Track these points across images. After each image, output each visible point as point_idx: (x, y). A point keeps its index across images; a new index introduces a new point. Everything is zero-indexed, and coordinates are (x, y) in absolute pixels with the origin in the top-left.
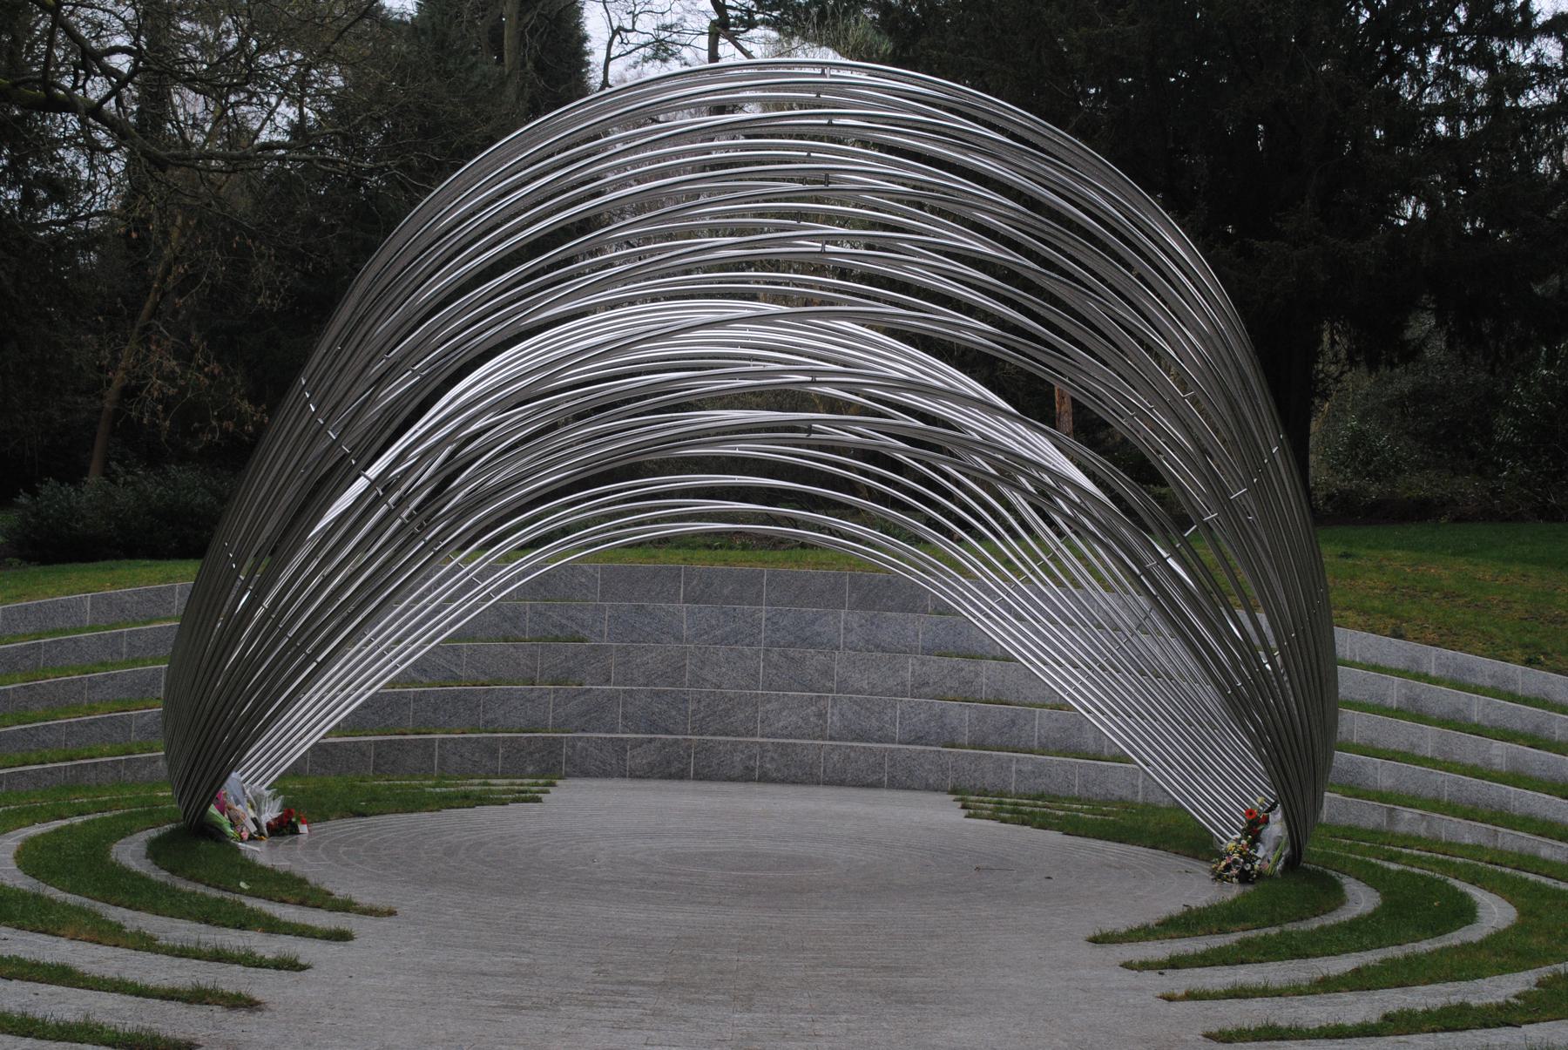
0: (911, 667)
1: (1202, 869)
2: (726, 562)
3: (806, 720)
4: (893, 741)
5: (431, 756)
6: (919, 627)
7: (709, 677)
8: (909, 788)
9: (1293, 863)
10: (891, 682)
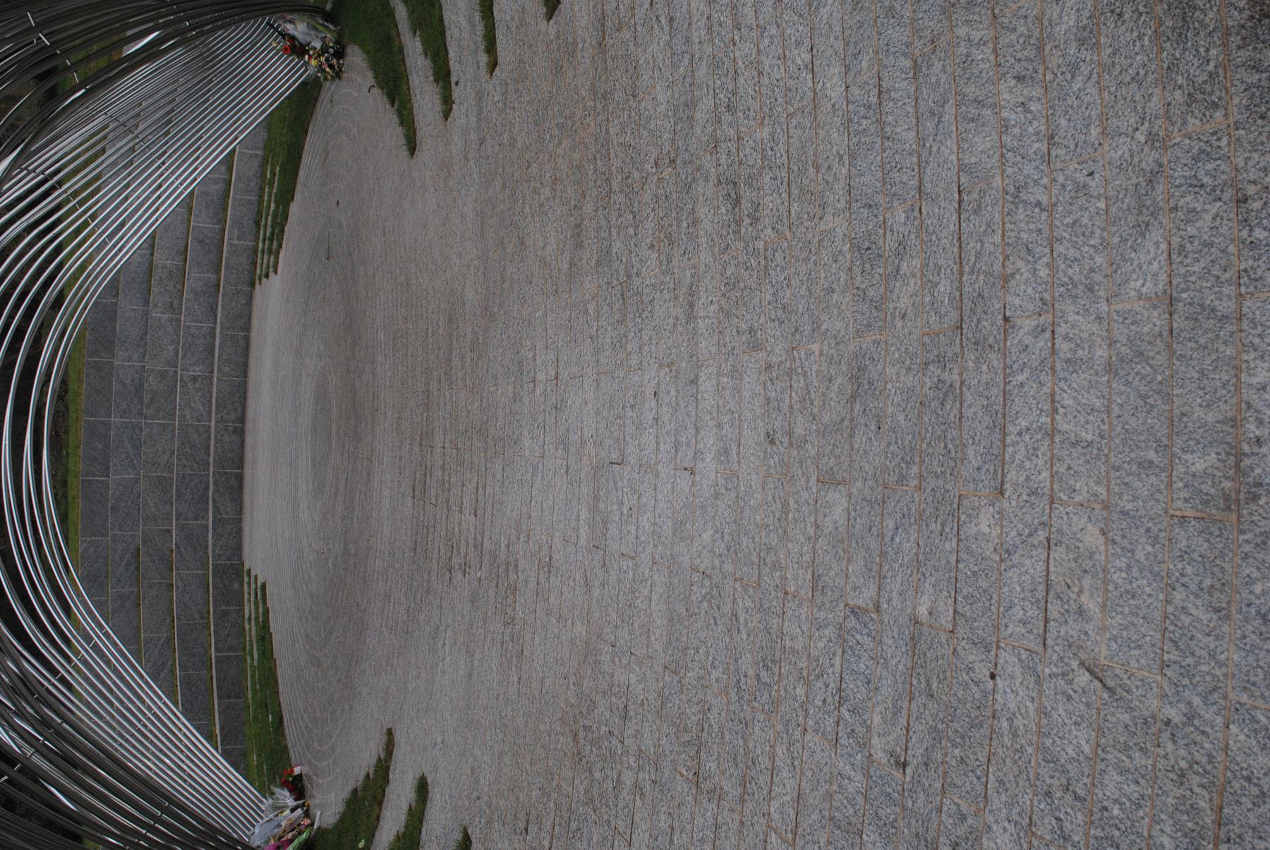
0: (158, 314)
1: (330, 90)
2: (77, 447)
4: (214, 329)
5: (228, 657)
6: (128, 307)
8: (250, 318)
9: (330, 17)
10: (170, 329)
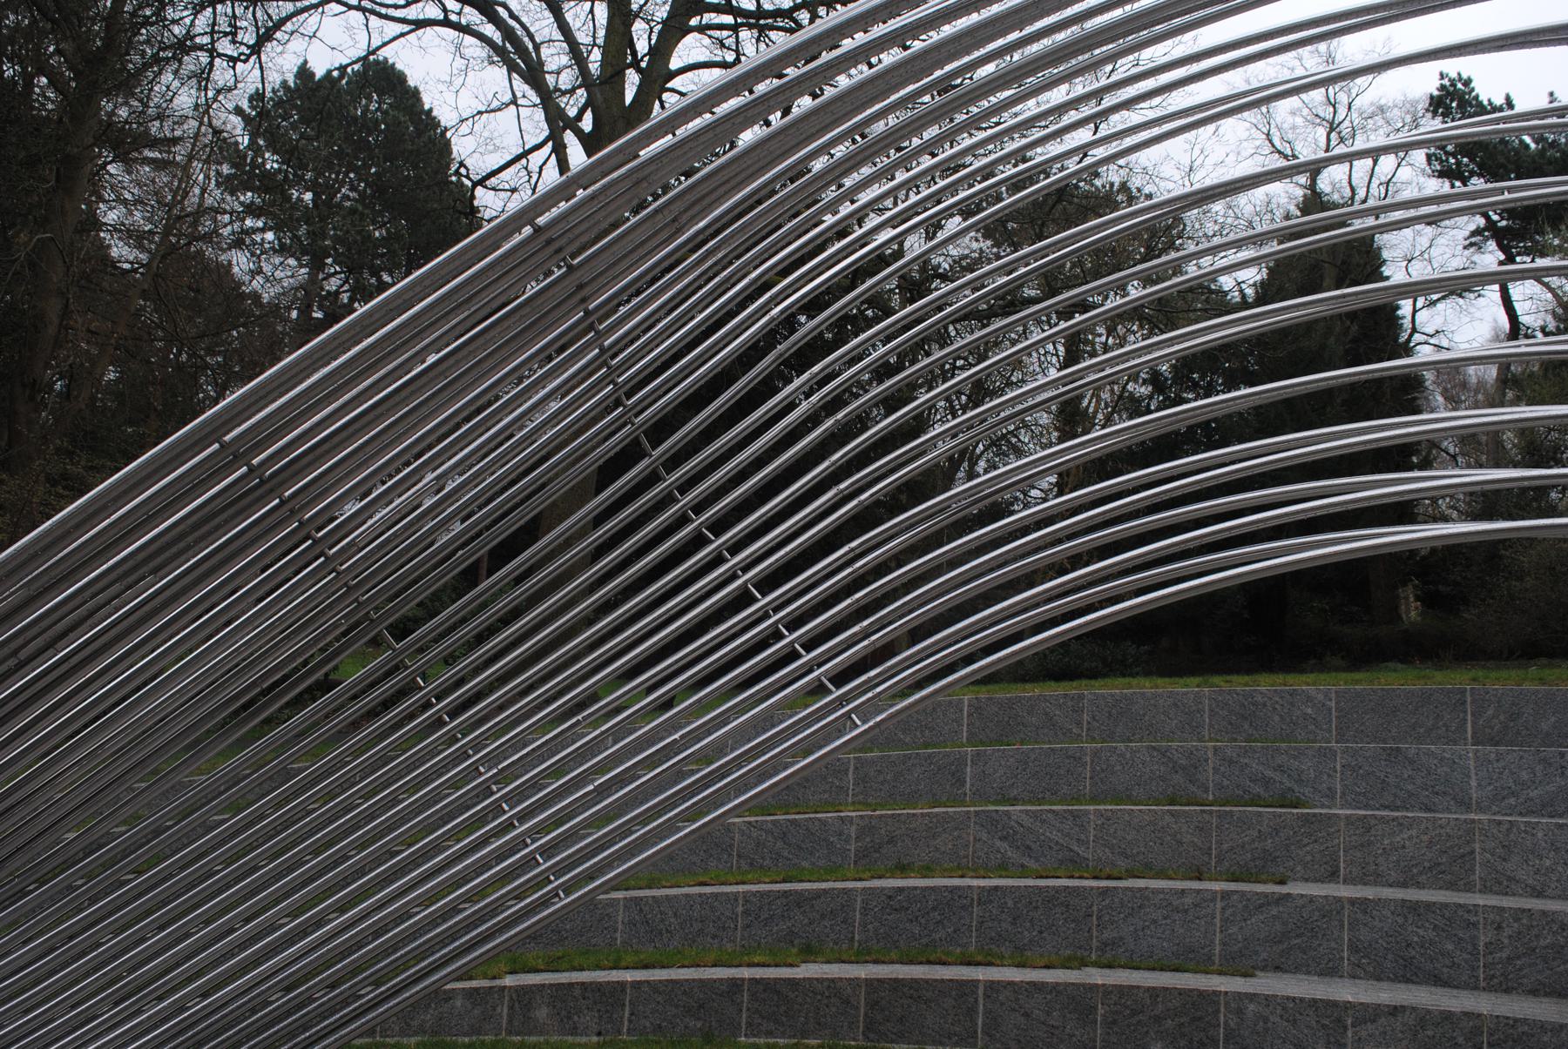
2: (1542, 681)
5: (972, 1011)
7: (1521, 874)
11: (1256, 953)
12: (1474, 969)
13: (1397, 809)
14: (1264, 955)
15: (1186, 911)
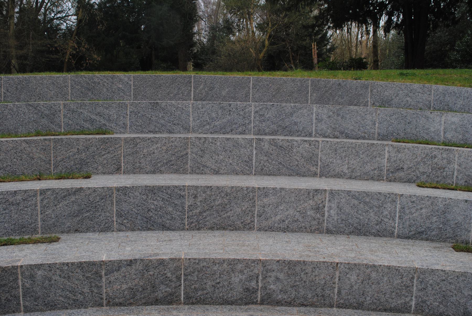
3: (303, 213)
7: (209, 164)
10: (368, 168)
11: (64, 224)
12: (182, 220)
13: (155, 132)
14: (68, 224)
15: (18, 204)
